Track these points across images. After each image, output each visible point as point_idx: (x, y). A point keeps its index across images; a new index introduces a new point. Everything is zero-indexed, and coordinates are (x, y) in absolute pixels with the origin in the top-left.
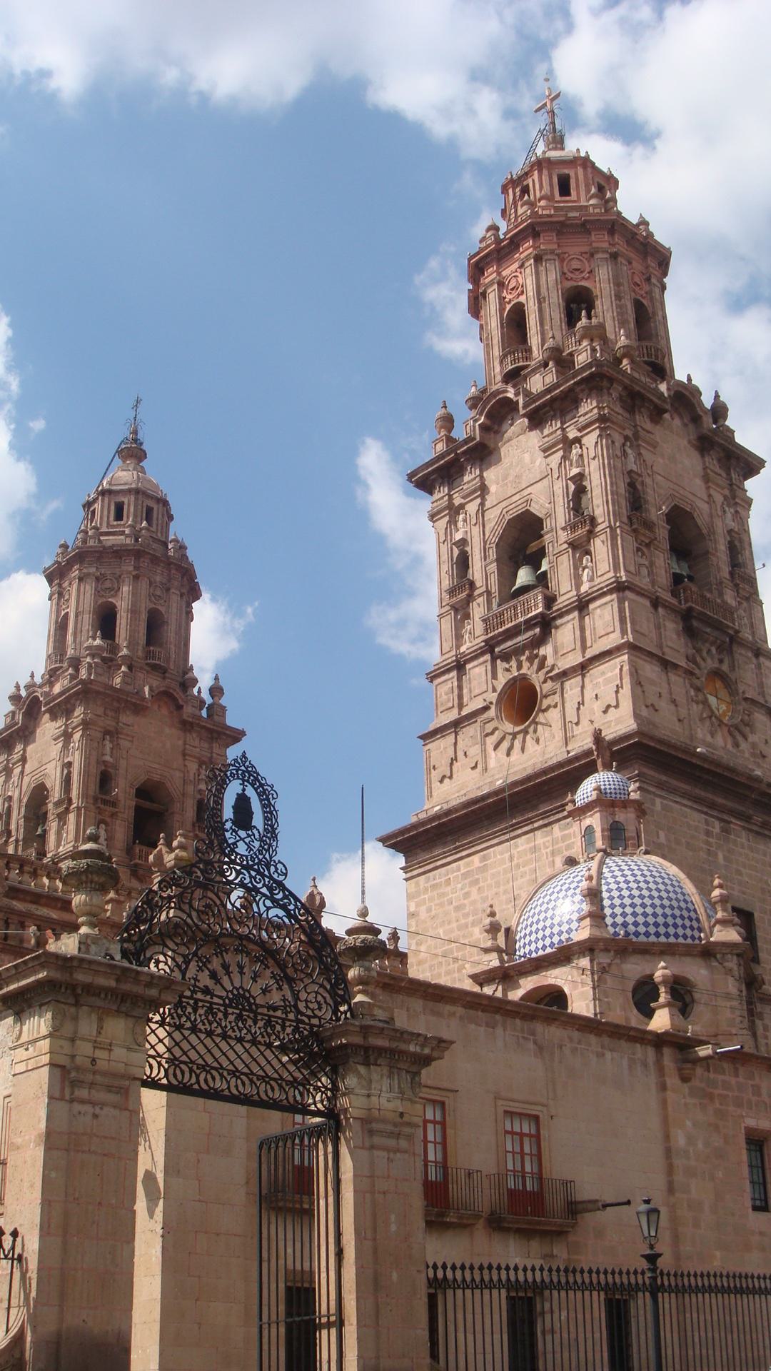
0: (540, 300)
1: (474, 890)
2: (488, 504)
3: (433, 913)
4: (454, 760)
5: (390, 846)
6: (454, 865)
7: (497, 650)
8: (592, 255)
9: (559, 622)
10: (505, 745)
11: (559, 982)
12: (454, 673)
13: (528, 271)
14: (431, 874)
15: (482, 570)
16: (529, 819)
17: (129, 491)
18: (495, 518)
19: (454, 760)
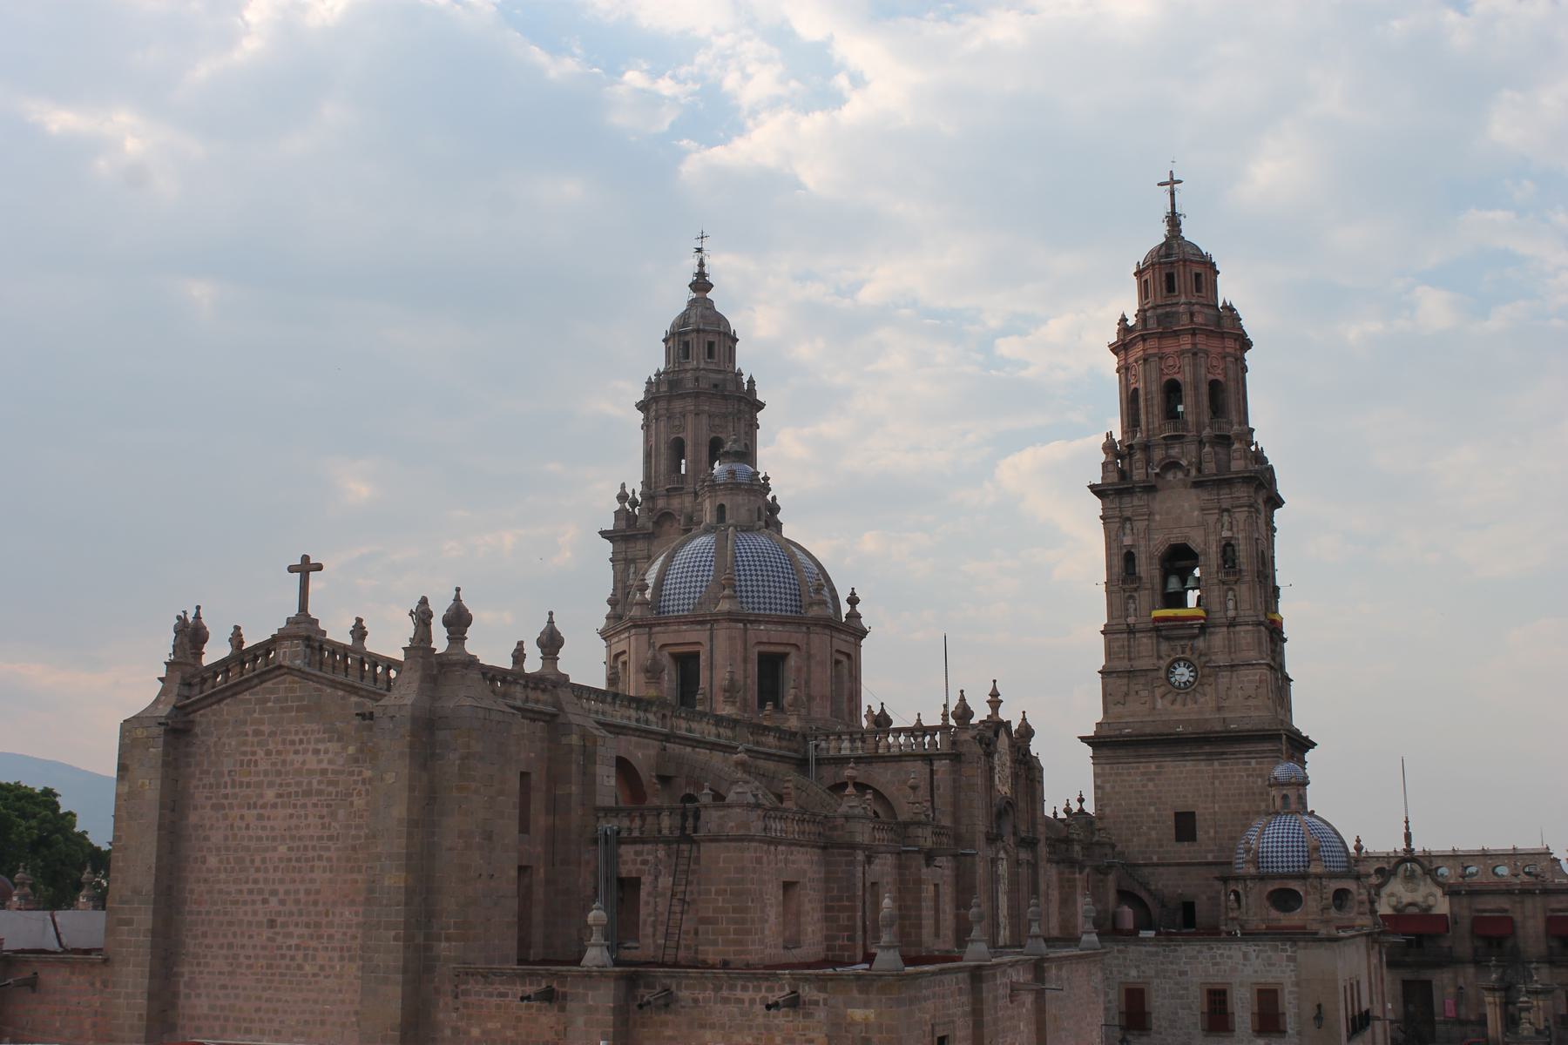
0: (1196, 388)
1: (1151, 785)
2: (1153, 525)
3: (1117, 789)
4: (1127, 694)
5: (1089, 744)
6: (1135, 765)
7: (1164, 633)
8: (1225, 357)
9: (1212, 629)
10: (1170, 697)
11: (1297, 888)
12: (1125, 635)
13: (1187, 360)
14: (1115, 766)
15: (1147, 568)
16: (1198, 753)
17: (719, 333)
18: (1159, 542)
19: (1127, 694)
